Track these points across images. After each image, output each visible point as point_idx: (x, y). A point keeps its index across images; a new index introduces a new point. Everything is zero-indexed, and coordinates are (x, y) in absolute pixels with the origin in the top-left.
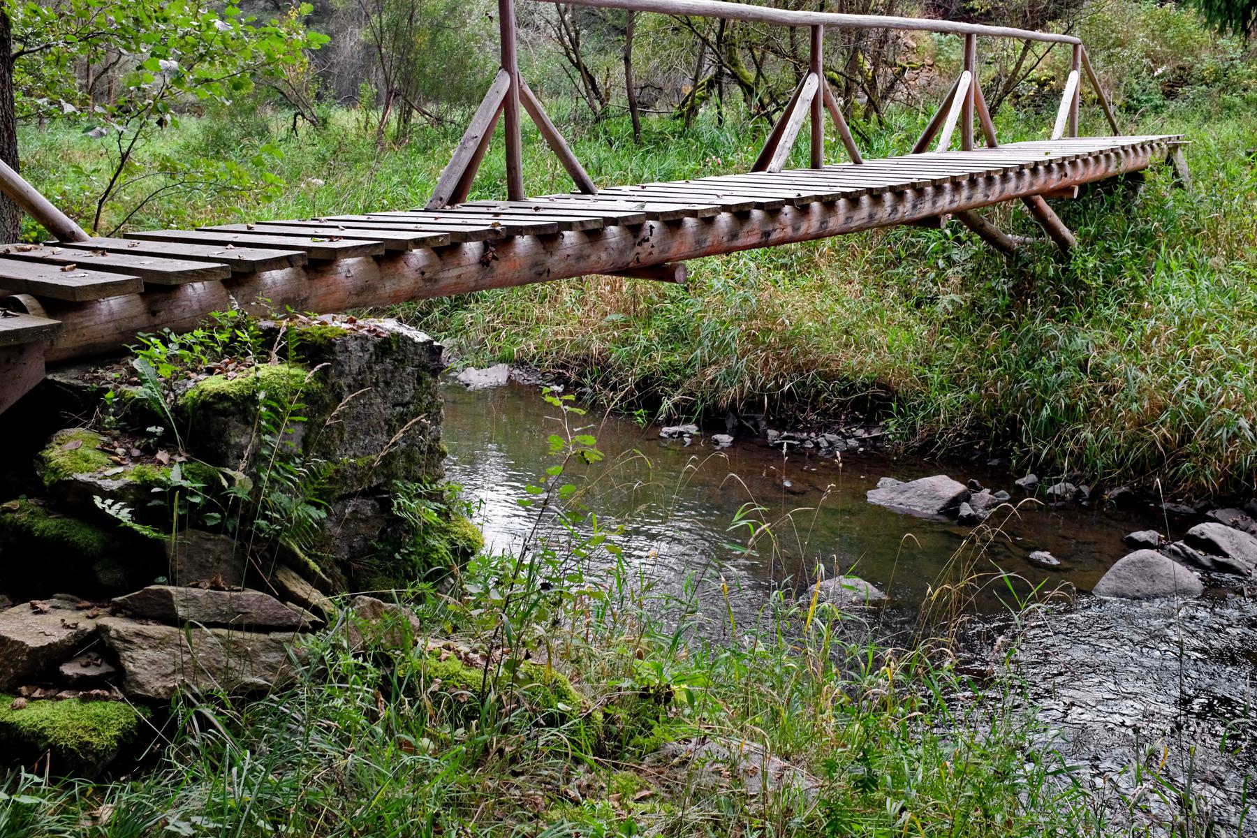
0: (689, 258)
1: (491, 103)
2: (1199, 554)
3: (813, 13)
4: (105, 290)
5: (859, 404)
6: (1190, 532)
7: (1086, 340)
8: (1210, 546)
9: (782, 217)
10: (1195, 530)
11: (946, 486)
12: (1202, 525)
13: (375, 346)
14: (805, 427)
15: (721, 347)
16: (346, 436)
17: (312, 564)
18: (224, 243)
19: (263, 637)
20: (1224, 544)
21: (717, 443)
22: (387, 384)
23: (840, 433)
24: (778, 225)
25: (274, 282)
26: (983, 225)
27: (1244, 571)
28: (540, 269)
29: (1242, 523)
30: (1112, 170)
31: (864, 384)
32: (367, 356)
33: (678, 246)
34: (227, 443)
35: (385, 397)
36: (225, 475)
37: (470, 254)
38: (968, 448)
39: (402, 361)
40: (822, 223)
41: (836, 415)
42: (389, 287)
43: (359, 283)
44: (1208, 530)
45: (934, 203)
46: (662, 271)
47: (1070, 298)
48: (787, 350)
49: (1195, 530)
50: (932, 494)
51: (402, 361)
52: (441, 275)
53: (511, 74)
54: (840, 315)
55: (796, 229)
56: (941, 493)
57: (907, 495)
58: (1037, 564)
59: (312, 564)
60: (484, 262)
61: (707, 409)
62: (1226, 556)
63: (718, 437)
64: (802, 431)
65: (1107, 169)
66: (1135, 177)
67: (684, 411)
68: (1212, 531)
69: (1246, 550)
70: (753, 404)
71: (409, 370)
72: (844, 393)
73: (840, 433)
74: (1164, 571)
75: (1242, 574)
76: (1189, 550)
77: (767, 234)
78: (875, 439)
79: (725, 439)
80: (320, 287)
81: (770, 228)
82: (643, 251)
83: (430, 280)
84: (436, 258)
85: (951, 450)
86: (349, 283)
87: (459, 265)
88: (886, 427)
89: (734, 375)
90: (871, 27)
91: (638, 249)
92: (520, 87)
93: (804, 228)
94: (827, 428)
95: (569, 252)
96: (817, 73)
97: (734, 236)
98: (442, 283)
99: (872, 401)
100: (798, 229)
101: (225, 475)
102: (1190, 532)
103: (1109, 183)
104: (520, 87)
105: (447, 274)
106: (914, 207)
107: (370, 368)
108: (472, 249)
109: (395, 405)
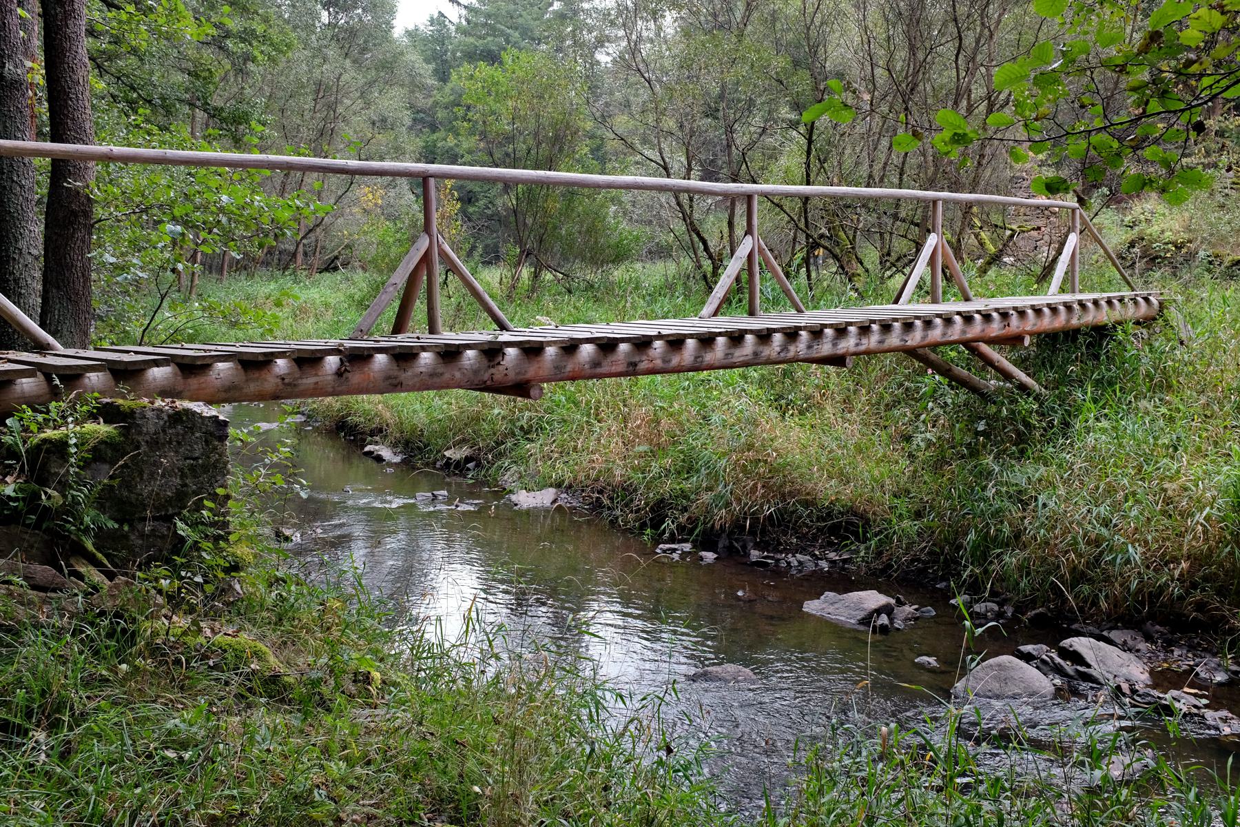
0: (548, 381)
1: (411, 259)
2: (1068, 666)
3: (745, 185)
4: (22, 373)
5: (834, 529)
6: (1061, 644)
7: (1023, 474)
8: (1076, 658)
9: (651, 353)
10: (1066, 643)
11: (873, 599)
12: (1075, 639)
13: (169, 416)
14: (785, 549)
15: (714, 476)
16: (145, 476)
17: (100, 555)
18: (128, 352)
19: (42, 594)
20: (1089, 656)
21: (702, 559)
22: (179, 443)
23: (813, 555)
24: (644, 358)
25: (155, 379)
26: (950, 370)
27: (1102, 681)
28: (395, 382)
29: (1130, 642)
30: (1075, 322)
31: (840, 513)
32: (162, 423)
33: (531, 371)
34: (49, 472)
35: (176, 452)
36: (46, 493)
37: (328, 367)
38: (922, 572)
39: (191, 428)
40: (696, 358)
41: (815, 538)
42: (252, 388)
43: (227, 383)
44: (1080, 644)
45: (835, 345)
46: (521, 388)
47: (1020, 441)
48: (778, 483)
49: (1066, 643)
50: (858, 606)
51: (191, 428)
52: (300, 381)
53: (430, 236)
54: (835, 448)
55: (666, 361)
56: (865, 606)
57: (836, 606)
58: (921, 666)
59: (100, 555)
60: (339, 373)
61: (704, 532)
62: (1089, 666)
63: (703, 553)
64: (781, 552)
65: (1068, 321)
66: (1101, 332)
67: (683, 533)
68: (1081, 645)
69: (1109, 662)
70: (738, 526)
71: (198, 435)
72: (820, 519)
73: (813, 555)
74: (1017, 675)
75: (1099, 683)
76: (1058, 660)
77: (635, 365)
78: (845, 561)
79: (709, 556)
80: (194, 382)
81: (637, 359)
82: (498, 373)
83: (289, 384)
84: (296, 368)
85: (907, 573)
86: (218, 383)
87: (316, 375)
88: (857, 552)
89: (716, 501)
90: (814, 196)
91: (493, 370)
92: (439, 246)
93: (675, 361)
94: (803, 550)
95: (423, 370)
96: (752, 235)
97: (596, 364)
98: (302, 388)
99: (844, 525)
100: (670, 361)
101: (46, 493)
102: (1061, 644)
103: (1071, 335)
104: (439, 246)
105: (304, 381)
106: (809, 347)
107: (164, 431)
108: (332, 361)
109: (186, 459)
